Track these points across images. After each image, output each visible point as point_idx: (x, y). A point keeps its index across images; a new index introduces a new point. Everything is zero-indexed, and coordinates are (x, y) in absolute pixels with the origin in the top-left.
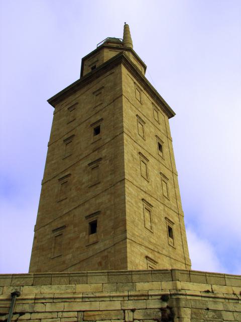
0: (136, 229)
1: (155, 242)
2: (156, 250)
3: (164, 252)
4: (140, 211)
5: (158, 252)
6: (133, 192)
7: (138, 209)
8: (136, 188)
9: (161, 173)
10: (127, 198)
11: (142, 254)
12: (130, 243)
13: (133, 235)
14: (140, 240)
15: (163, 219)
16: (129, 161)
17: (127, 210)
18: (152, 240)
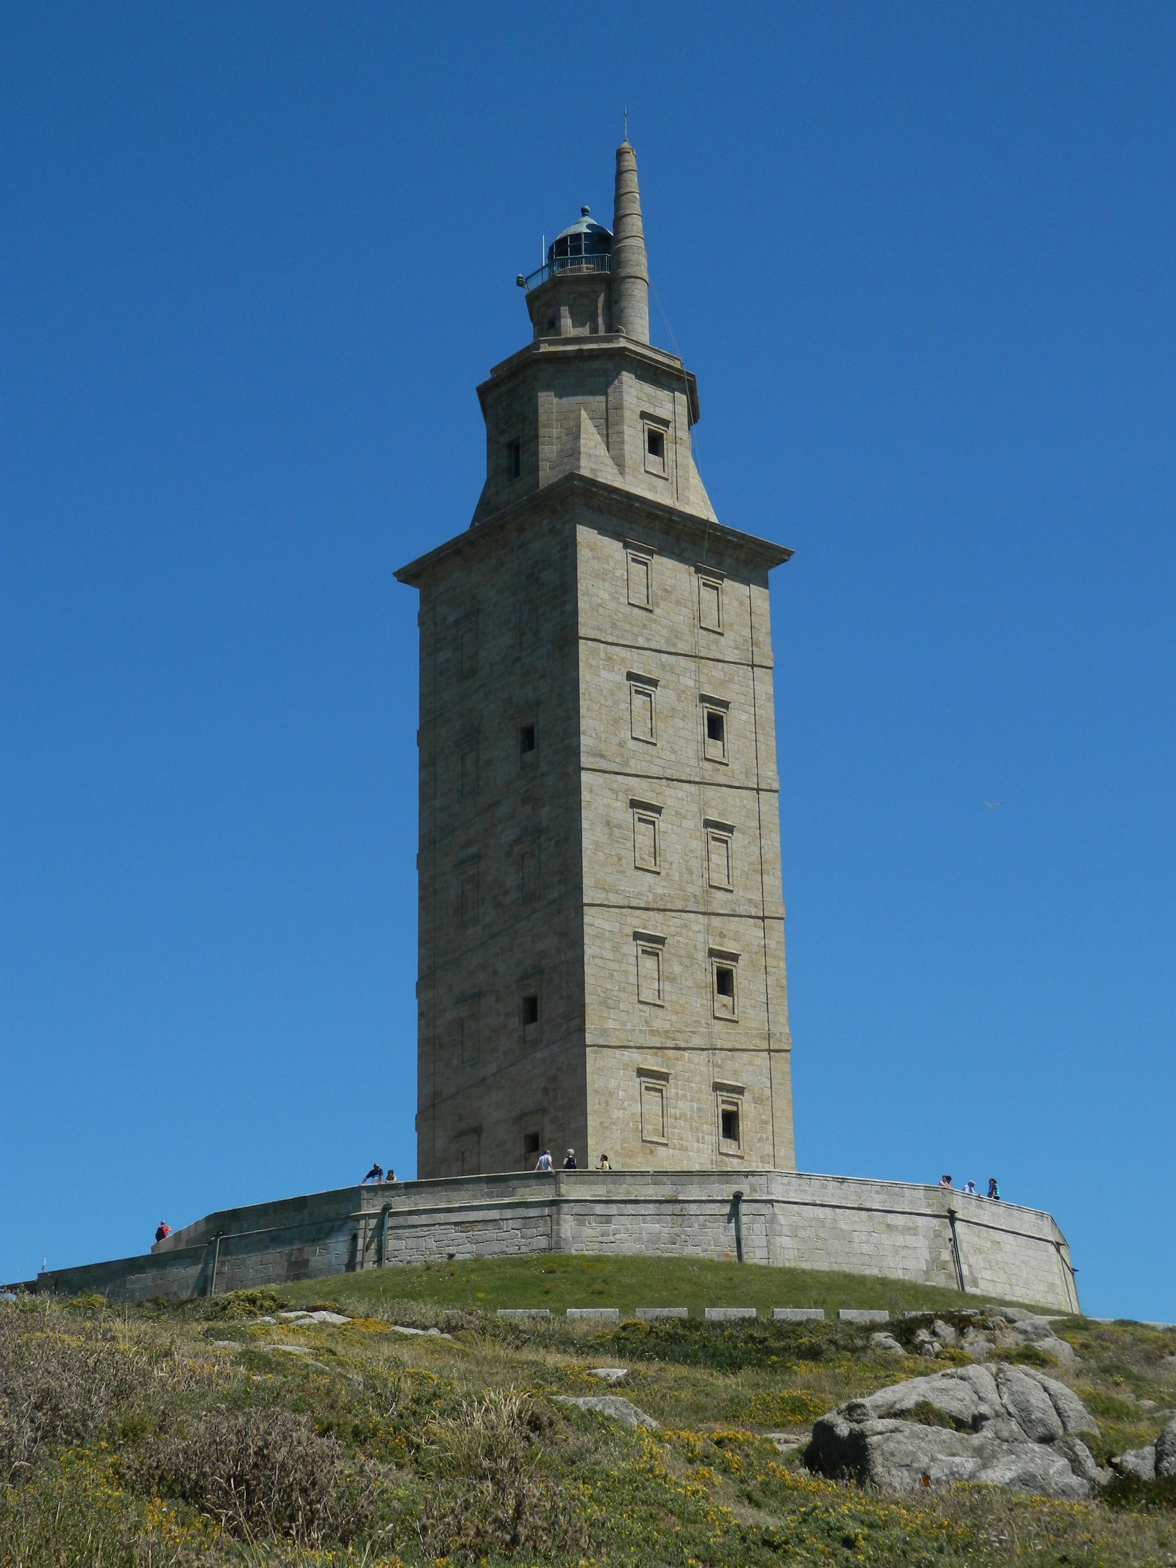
0: (613, 1014)
1: (667, 1026)
2: (670, 1044)
3: (696, 1041)
4: (624, 967)
5: (677, 1048)
6: (607, 926)
7: (620, 962)
8: (616, 910)
9: (708, 824)
10: (588, 951)
11: (626, 1066)
12: (595, 1053)
13: (604, 1032)
14: (622, 1036)
15: (701, 956)
16: (597, 846)
17: (589, 980)
18: (657, 1024)
